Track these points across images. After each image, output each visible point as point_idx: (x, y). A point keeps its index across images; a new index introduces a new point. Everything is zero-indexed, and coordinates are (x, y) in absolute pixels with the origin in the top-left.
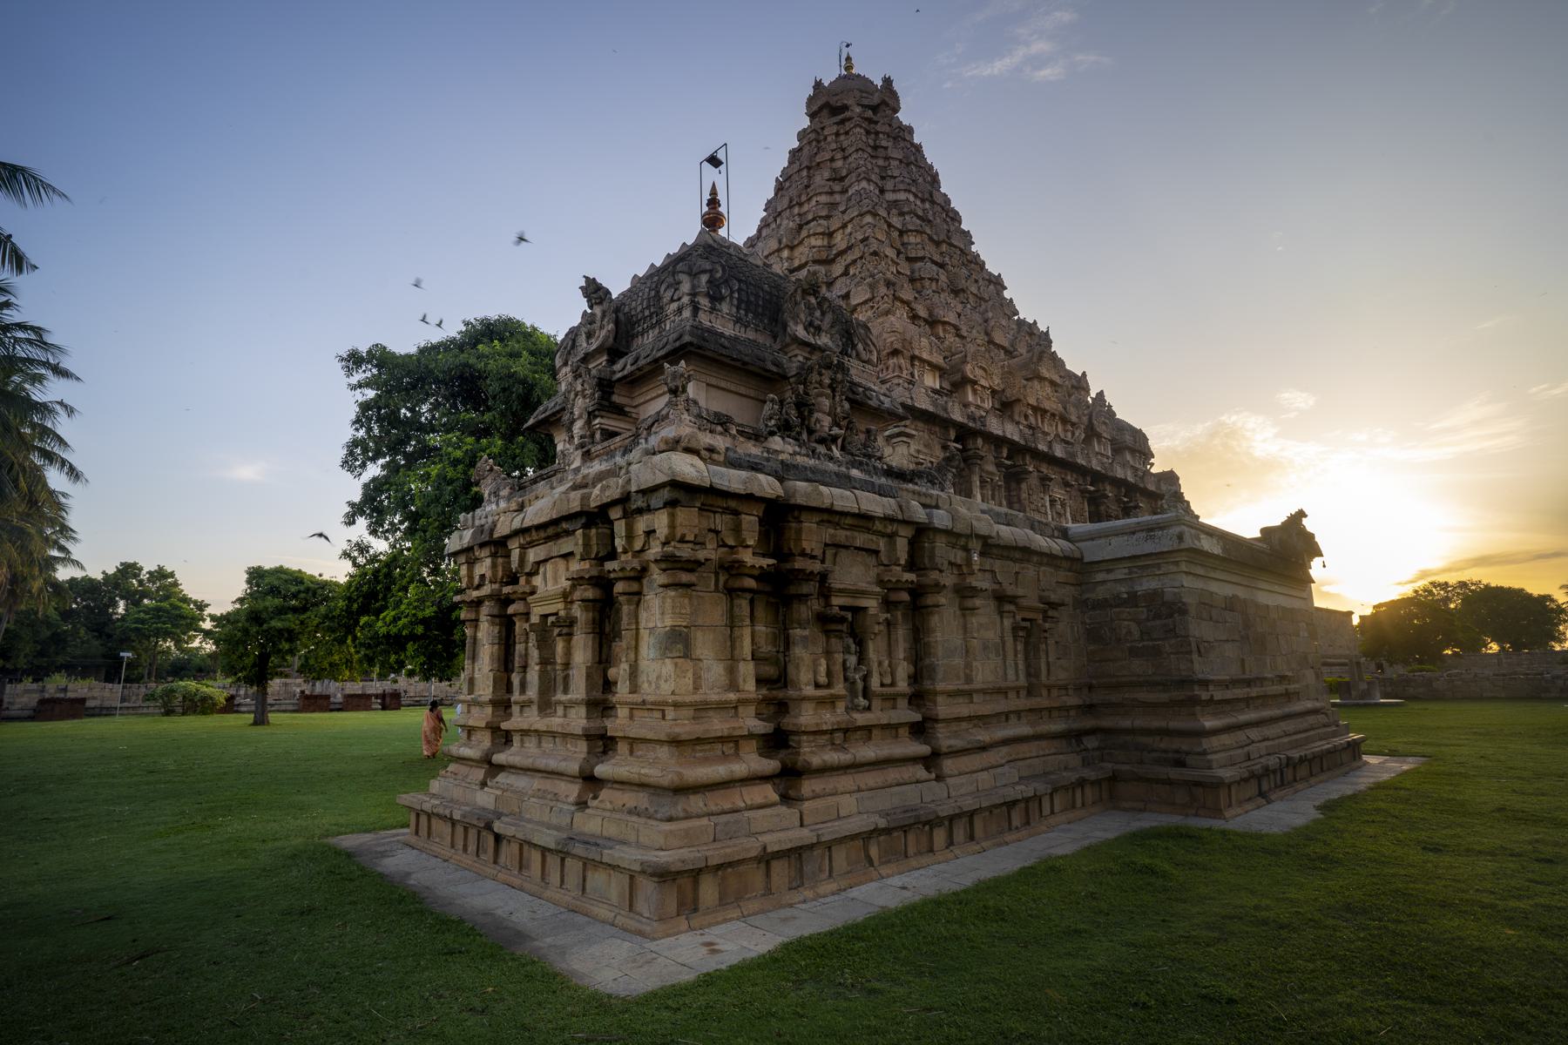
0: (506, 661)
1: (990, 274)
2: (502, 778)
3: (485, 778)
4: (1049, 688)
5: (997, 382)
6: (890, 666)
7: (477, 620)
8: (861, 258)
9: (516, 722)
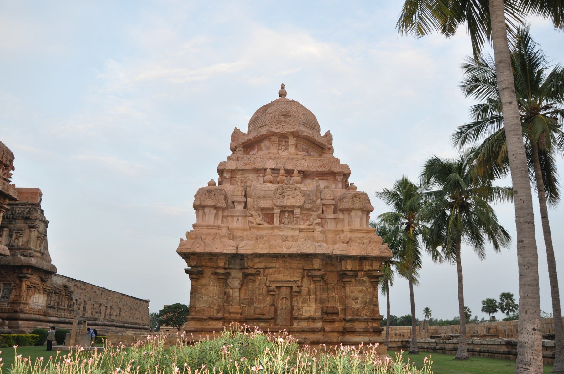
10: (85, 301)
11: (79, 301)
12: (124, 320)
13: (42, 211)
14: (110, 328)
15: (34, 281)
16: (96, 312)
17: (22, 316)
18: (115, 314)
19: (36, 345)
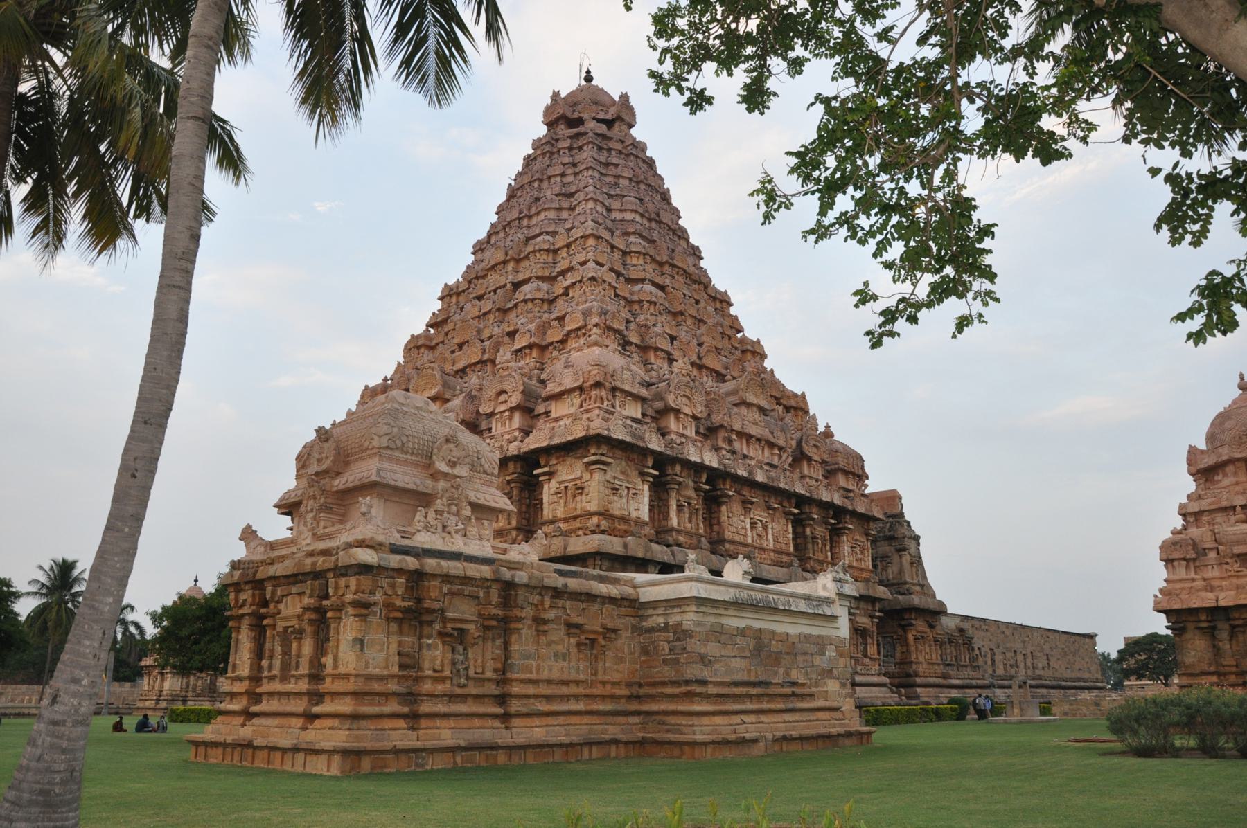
0: (259, 653)
1: (717, 291)
2: (255, 721)
3: (245, 721)
4: (604, 683)
5: (700, 410)
8: (580, 281)
9: (266, 687)
10: (992, 650)
11: (983, 650)
12: (1057, 675)
13: (908, 523)
14: (1038, 690)
15: (921, 629)
16: (1011, 666)
17: (918, 680)
18: (1040, 665)
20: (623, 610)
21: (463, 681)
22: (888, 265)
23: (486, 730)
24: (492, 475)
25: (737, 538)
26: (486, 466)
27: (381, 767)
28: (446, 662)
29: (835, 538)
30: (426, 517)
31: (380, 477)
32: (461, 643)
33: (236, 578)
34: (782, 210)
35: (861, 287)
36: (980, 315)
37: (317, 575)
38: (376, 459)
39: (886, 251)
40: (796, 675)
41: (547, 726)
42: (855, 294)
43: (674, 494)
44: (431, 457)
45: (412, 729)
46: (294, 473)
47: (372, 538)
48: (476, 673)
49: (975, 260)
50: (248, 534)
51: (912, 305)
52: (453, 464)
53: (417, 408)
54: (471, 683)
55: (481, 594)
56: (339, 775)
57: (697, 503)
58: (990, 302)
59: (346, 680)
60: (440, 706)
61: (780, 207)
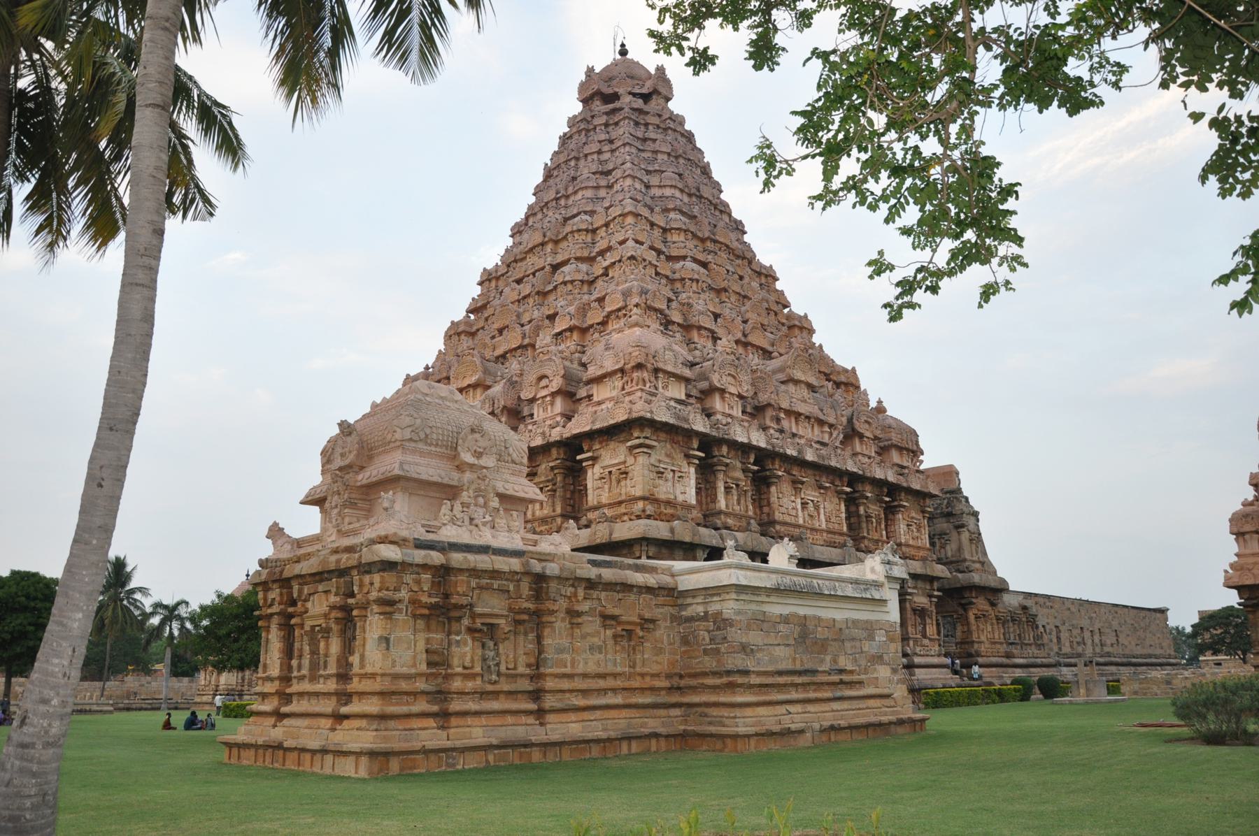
0: (288, 652)
1: (762, 266)
2: (286, 722)
3: (276, 722)
4: (643, 675)
5: (746, 389)
6: (514, 657)
7: (269, 627)
8: (620, 261)
9: (296, 687)
10: (1057, 627)
11: (1048, 627)
12: (1127, 652)
13: (967, 499)
14: (1107, 668)
15: (981, 607)
18: (1109, 642)
19: (1022, 700)
20: (661, 599)
21: (494, 677)
22: (906, 231)
23: (519, 728)
24: (521, 464)
25: (788, 519)
26: (514, 456)
27: (411, 768)
28: (476, 658)
29: (891, 516)
30: (452, 510)
31: (403, 470)
32: (492, 639)
33: (263, 578)
34: (784, 177)
35: (875, 256)
36: (1007, 282)
37: (342, 572)
38: (399, 452)
39: (900, 216)
40: (844, 662)
41: (583, 721)
42: (870, 264)
43: (721, 476)
44: (456, 448)
45: (443, 728)
46: (320, 468)
47: (395, 534)
48: (507, 669)
49: (999, 222)
50: (275, 532)
51: (932, 274)
52: (478, 455)
53: (442, 397)
54: (503, 679)
55: (511, 588)
56: (366, 777)
57: (746, 484)
58: (1018, 267)
59: (372, 680)
60: (470, 703)
61: (780, 173)
